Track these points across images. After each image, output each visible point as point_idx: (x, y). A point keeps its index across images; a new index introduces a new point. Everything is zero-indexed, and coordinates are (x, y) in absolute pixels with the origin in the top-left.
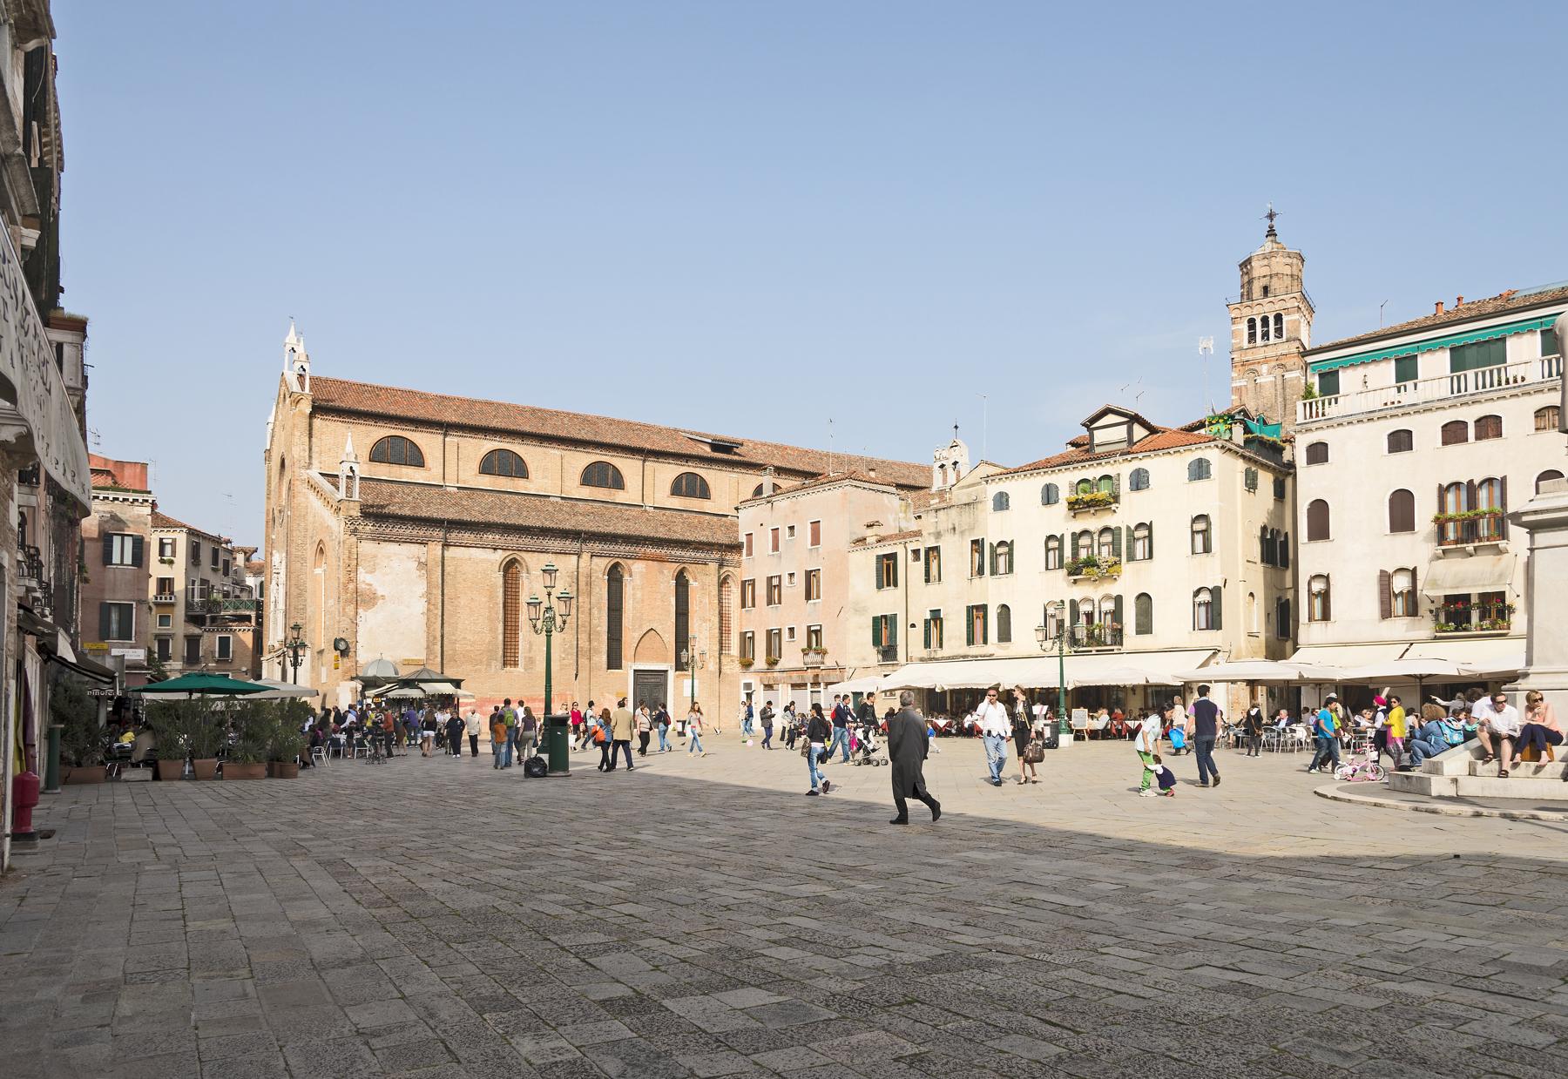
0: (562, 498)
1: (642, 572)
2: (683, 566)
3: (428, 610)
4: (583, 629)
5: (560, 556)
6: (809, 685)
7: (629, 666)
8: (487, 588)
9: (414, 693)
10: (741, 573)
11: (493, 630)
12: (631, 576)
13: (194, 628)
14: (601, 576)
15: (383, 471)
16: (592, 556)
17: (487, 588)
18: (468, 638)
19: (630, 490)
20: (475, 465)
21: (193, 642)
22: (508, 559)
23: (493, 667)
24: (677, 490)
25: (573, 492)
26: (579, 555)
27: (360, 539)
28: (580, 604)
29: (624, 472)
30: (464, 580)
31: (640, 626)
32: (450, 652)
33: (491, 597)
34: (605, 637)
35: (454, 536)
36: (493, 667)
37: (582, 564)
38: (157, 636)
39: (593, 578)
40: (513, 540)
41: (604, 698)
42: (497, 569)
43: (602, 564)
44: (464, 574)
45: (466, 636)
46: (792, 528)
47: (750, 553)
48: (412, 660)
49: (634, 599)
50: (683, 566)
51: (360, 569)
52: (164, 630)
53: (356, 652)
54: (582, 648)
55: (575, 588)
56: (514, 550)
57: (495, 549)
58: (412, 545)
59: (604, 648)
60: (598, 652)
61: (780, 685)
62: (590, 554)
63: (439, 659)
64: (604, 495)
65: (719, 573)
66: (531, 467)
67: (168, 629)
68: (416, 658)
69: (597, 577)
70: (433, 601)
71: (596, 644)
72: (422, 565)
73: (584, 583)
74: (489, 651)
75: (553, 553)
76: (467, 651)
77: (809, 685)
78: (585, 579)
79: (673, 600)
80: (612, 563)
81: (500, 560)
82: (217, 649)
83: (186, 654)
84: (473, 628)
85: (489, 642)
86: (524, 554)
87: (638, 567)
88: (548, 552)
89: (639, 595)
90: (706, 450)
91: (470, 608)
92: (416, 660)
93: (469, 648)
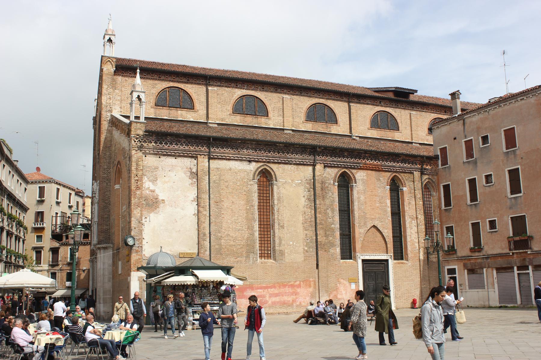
0: (293, 130)
1: (362, 180)
2: (394, 174)
3: (198, 211)
4: (321, 226)
5: (301, 167)
6: (515, 268)
7: (361, 256)
8: (245, 193)
9: (188, 280)
10: (438, 180)
11: (250, 228)
12: (356, 183)
13: (56, 243)
14: (332, 182)
15: (164, 113)
16: (325, 167)
17: (245, 193)
18: (231, 235)
19: (341, 125)
20: (230, 108)
21: (55, 251)
22: (260, 170)
23: (251, 259)
24: (375, 123)
25: (300, 126)
26: (314, 166)
27: (145, 154)
28: (318, 206)
29: (336, 111)
30: (227, 187)
31: (365, 224)
32: (217, 247)
33: (249, 201)
34: (338, 234)
35: (216, 151)
36: (251, 259)
37: (317, 173)
38: (34, 248)
39: (327, 185)
40: (263, 155)
41: (340, 283)
42: (252, 176)
43: (332, 173)
44: (227, 182)
45: (229, 233)
46: (485, 139)
47: (445, 162)
48: (187, 254)
49: (359, 201)
50: (394, 174)
51: (145, 179)
52: (39, 244)
53: (141, 247)
54: (320, 242)
55: (313, 193)
56: (264, 162)
57: (250, 161)
58: (186, 159)
59: (338, 242)
60: (332, 245)
61: (485, 270)
62: (323, 165)
63: (208, 253)
64: (323, 128)
65: (421, 180)
66: (270, 109)
67: (41, 244)
68: (189, 252)
69: (330, 184)
70: (202, 205)
71: (331, 238)
72: (195, 175)
73: (320, 188)
74: (248, 245)
75: (294, 164)
76: (231, 246)
77: (515, 268)
78: (320, 185)
79: (388, 202)
80: (341, 172)
81: (254, 170)
82: (69, 256)
83: (51, 260)
84: (234, 227)
85: (248, 239)
86: (272, 165)
87: (360, 175)
88: (291, 164)
89: (362, 198)
90: (391, 95)
91: (232, 210)
92: (190, 254)
93: (232, 243)
